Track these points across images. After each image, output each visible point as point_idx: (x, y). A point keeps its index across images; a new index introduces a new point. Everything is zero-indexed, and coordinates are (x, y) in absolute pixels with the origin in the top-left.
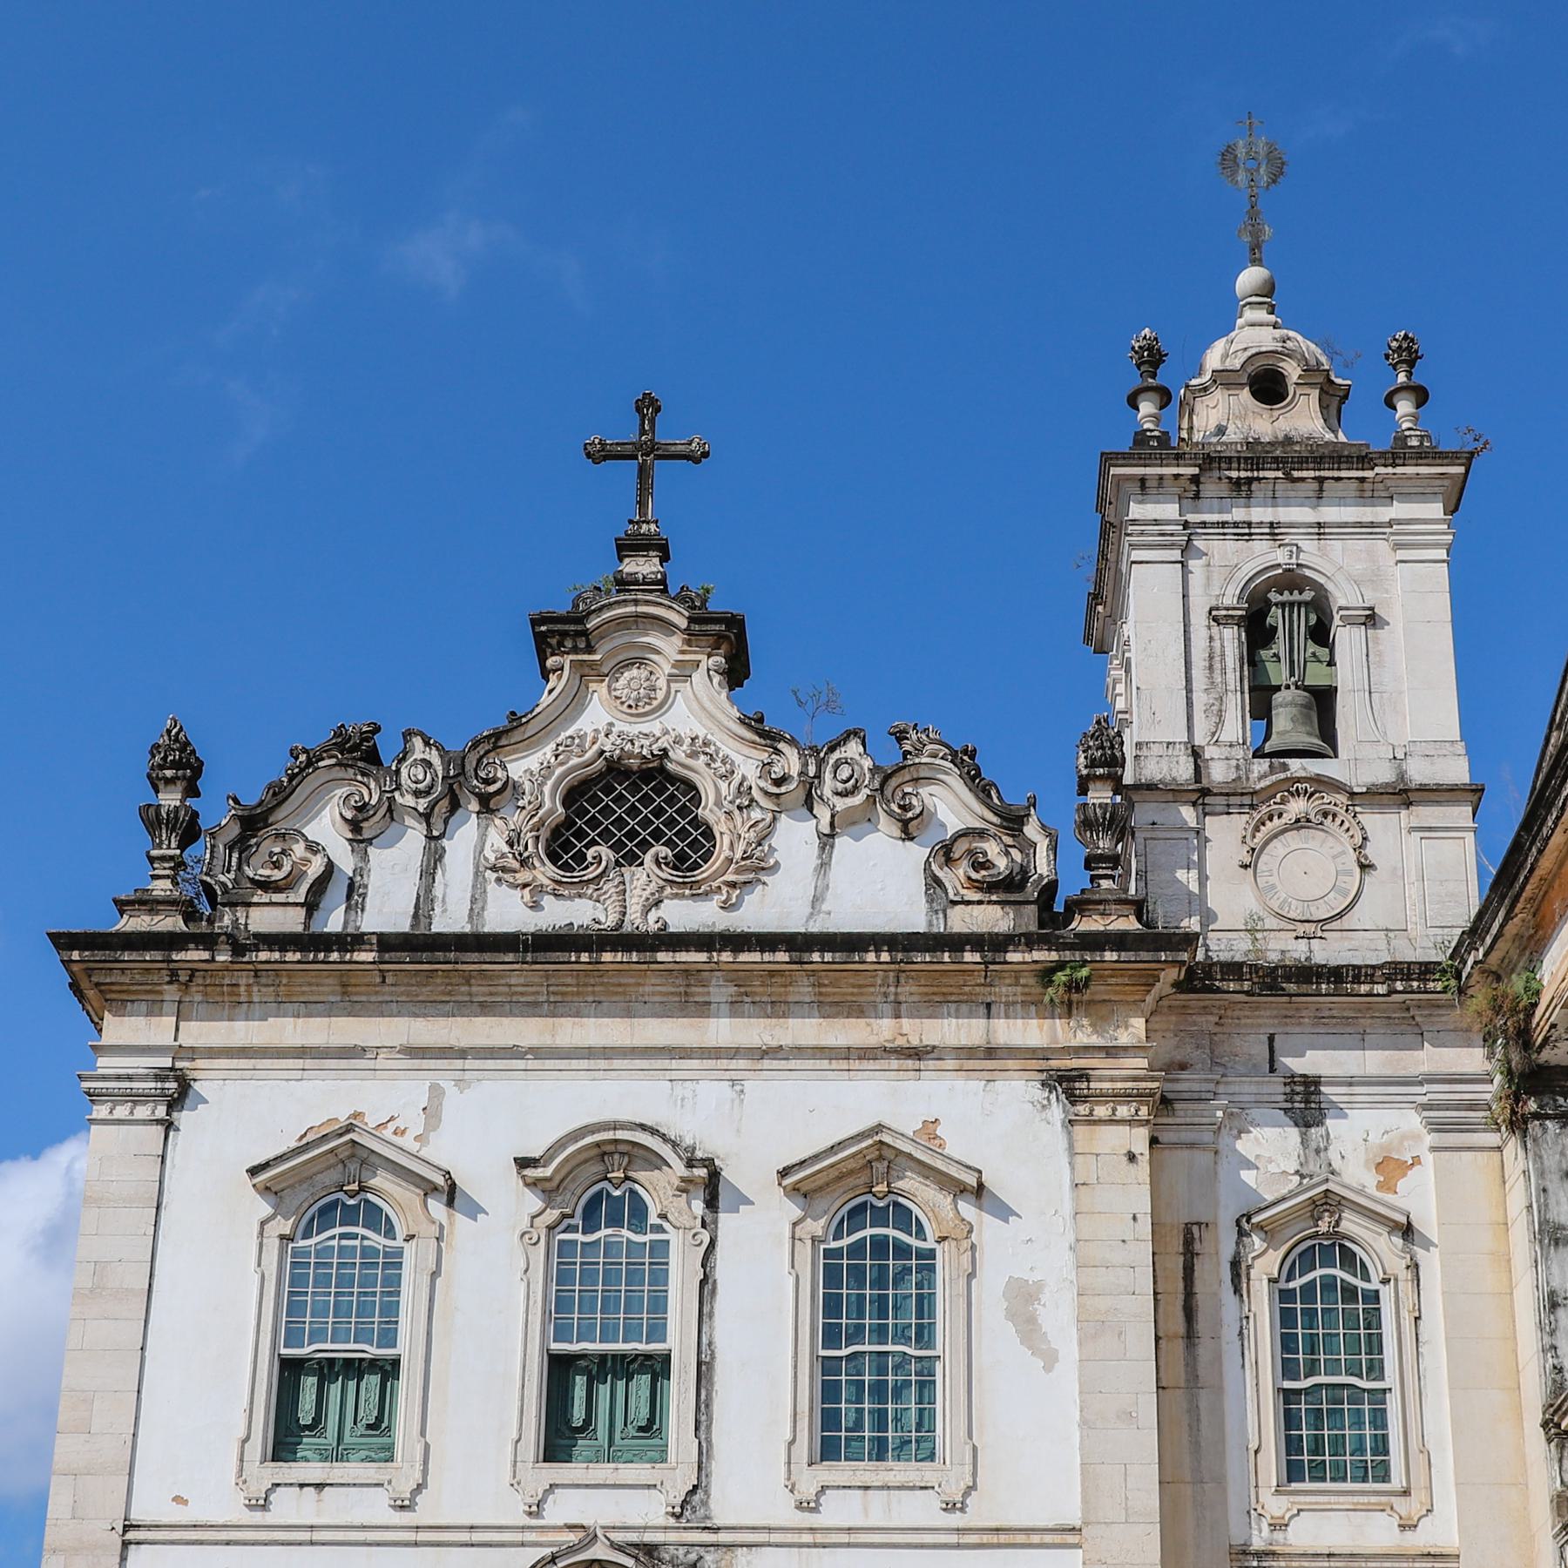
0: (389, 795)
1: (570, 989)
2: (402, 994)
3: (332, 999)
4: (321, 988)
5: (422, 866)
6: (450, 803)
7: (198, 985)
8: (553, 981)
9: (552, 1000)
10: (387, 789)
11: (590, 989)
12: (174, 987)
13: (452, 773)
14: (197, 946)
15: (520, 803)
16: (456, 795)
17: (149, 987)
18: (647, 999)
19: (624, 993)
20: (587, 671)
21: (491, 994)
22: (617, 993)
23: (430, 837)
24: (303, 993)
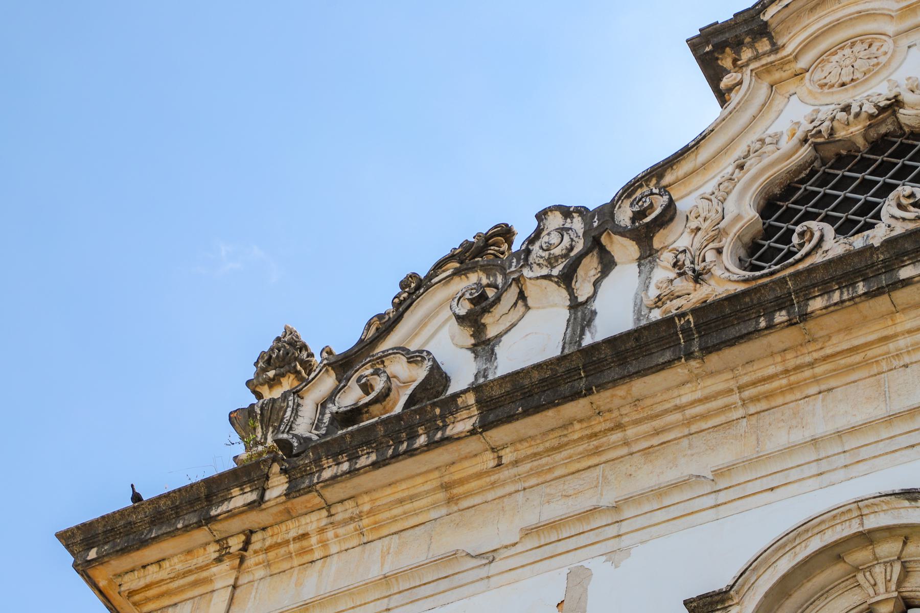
0: (515, 276)
1: (776, 384)
2: (529, 475)
3: (433, 514)
4: (417, 504)
5: (564, 338)
6: (601, 261)
7: (256, 552)
8: (745, 380)
9: (752, 409)
10: (513, 269)
11: (808, 373)
12: (225, 566)
13: (595, 224)
14: (242, 490)
15: (693, 224)
16: (609, 253)
17: (191, 578)
18: (906, 359)
19: (866, 363)
20: (777, 75)
21: (657, 432)
22: (852, 368)
23: (575, 306)
24: (394, 519)
